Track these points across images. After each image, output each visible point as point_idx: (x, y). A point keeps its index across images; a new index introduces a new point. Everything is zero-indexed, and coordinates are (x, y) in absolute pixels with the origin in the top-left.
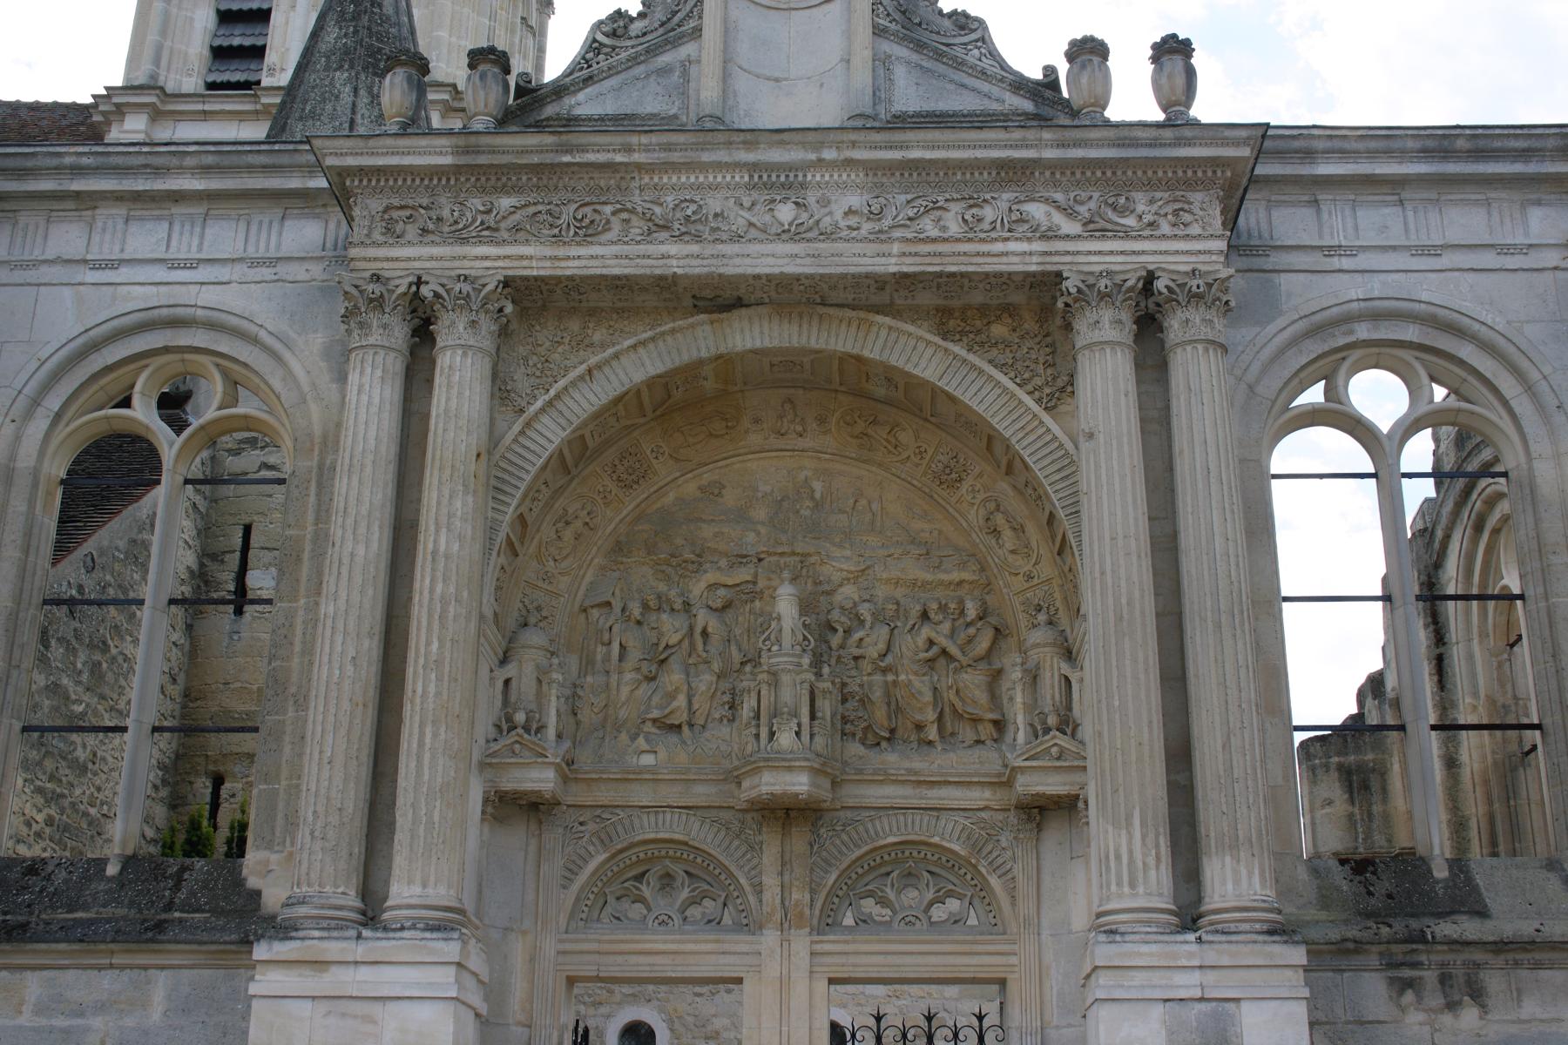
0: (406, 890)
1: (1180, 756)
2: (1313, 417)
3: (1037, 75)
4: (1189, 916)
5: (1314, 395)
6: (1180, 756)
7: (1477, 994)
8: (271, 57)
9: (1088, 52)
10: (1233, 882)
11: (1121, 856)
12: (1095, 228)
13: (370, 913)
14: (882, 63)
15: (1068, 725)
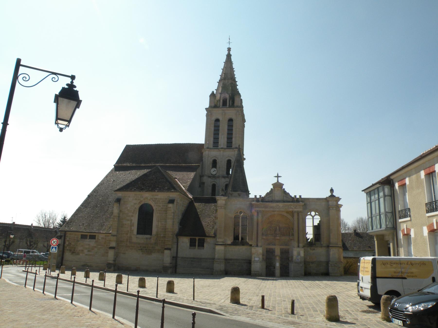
0: (259, 244)
1: (298, 238)
2: (309, 215)
3: (293, 196)
4: (298, 247)
5: (309, 213)
6: (298, 238)
7: (314, 249)
8: (219, 144)
9: (295, 196)
10: (301, 245)
11: (296, 244)
12: (295, 208)
13: (257, 246)
14: (283, 196)
15: (293, 235)
